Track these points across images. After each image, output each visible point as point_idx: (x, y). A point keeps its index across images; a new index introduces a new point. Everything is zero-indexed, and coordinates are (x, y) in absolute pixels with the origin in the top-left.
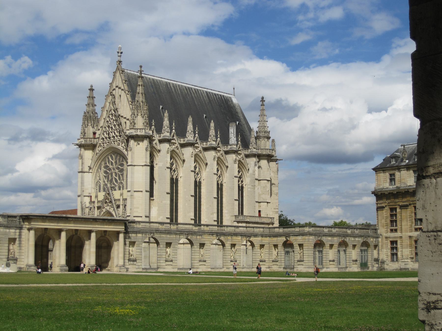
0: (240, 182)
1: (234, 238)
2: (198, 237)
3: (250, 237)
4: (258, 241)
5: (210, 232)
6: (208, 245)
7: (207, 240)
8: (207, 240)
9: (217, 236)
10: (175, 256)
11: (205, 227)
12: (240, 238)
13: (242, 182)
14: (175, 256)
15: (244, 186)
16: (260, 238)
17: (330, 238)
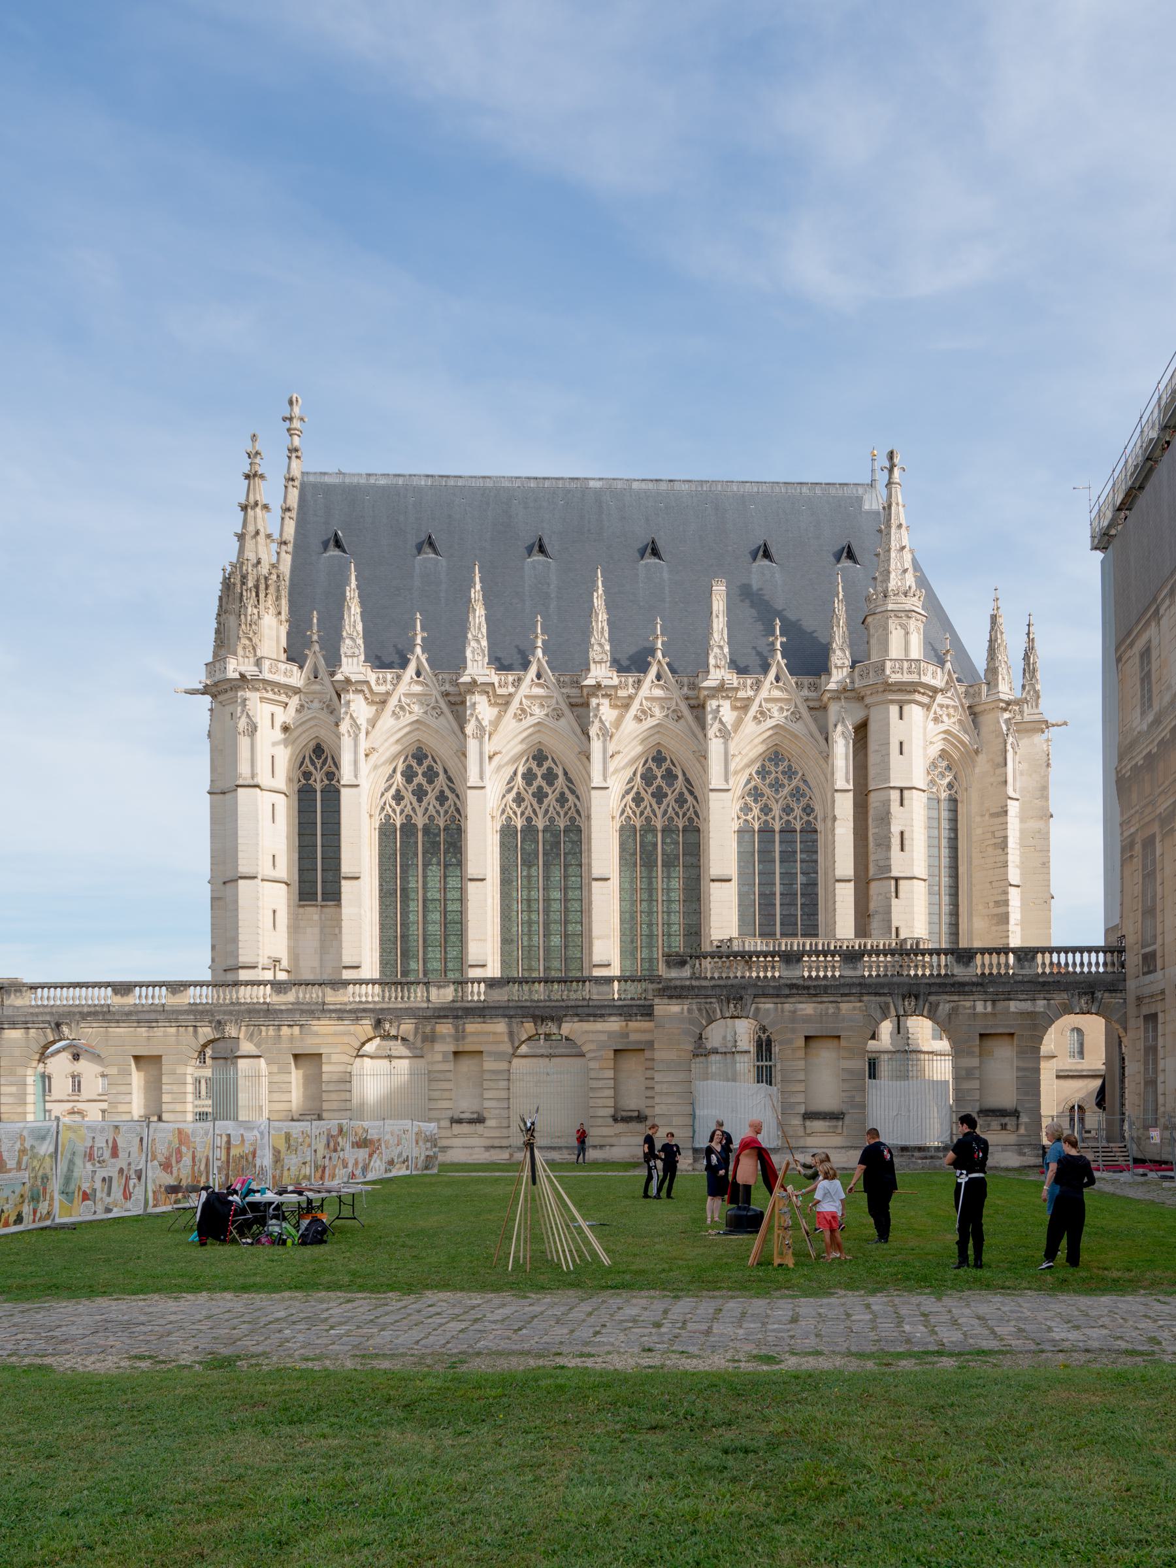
0: (798, 812)
1: (471, 1027)
2: (285, 1030)
3: (559, 1020)
4: (604, 1037)
5: (350, 1011)
6: (334, 1058)
7: (330, 1040)
8: (330, 1040)
9: (378, 1023)
10: (178, 1107)
11: (328, 990)
12: (500, 1027)
13: (808, 810)
14: (178, 1107)
15: (820, 827)
16: (614, 1025)
17: (807, 1008)
